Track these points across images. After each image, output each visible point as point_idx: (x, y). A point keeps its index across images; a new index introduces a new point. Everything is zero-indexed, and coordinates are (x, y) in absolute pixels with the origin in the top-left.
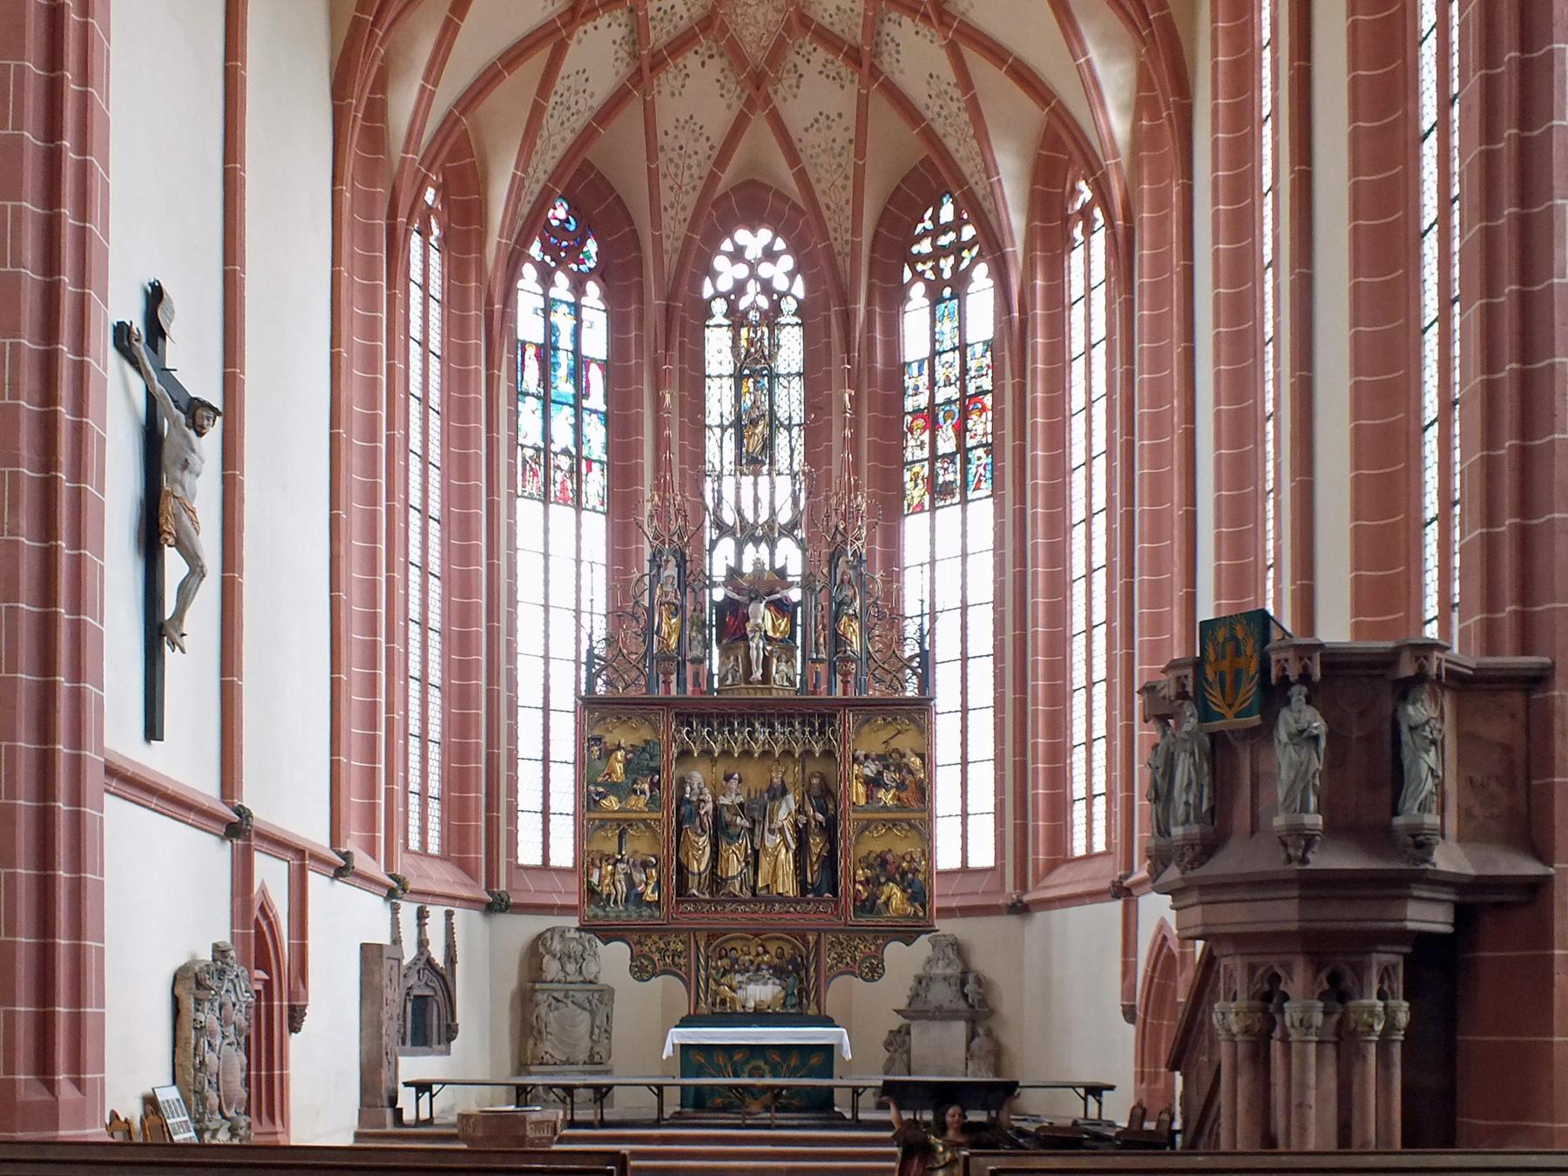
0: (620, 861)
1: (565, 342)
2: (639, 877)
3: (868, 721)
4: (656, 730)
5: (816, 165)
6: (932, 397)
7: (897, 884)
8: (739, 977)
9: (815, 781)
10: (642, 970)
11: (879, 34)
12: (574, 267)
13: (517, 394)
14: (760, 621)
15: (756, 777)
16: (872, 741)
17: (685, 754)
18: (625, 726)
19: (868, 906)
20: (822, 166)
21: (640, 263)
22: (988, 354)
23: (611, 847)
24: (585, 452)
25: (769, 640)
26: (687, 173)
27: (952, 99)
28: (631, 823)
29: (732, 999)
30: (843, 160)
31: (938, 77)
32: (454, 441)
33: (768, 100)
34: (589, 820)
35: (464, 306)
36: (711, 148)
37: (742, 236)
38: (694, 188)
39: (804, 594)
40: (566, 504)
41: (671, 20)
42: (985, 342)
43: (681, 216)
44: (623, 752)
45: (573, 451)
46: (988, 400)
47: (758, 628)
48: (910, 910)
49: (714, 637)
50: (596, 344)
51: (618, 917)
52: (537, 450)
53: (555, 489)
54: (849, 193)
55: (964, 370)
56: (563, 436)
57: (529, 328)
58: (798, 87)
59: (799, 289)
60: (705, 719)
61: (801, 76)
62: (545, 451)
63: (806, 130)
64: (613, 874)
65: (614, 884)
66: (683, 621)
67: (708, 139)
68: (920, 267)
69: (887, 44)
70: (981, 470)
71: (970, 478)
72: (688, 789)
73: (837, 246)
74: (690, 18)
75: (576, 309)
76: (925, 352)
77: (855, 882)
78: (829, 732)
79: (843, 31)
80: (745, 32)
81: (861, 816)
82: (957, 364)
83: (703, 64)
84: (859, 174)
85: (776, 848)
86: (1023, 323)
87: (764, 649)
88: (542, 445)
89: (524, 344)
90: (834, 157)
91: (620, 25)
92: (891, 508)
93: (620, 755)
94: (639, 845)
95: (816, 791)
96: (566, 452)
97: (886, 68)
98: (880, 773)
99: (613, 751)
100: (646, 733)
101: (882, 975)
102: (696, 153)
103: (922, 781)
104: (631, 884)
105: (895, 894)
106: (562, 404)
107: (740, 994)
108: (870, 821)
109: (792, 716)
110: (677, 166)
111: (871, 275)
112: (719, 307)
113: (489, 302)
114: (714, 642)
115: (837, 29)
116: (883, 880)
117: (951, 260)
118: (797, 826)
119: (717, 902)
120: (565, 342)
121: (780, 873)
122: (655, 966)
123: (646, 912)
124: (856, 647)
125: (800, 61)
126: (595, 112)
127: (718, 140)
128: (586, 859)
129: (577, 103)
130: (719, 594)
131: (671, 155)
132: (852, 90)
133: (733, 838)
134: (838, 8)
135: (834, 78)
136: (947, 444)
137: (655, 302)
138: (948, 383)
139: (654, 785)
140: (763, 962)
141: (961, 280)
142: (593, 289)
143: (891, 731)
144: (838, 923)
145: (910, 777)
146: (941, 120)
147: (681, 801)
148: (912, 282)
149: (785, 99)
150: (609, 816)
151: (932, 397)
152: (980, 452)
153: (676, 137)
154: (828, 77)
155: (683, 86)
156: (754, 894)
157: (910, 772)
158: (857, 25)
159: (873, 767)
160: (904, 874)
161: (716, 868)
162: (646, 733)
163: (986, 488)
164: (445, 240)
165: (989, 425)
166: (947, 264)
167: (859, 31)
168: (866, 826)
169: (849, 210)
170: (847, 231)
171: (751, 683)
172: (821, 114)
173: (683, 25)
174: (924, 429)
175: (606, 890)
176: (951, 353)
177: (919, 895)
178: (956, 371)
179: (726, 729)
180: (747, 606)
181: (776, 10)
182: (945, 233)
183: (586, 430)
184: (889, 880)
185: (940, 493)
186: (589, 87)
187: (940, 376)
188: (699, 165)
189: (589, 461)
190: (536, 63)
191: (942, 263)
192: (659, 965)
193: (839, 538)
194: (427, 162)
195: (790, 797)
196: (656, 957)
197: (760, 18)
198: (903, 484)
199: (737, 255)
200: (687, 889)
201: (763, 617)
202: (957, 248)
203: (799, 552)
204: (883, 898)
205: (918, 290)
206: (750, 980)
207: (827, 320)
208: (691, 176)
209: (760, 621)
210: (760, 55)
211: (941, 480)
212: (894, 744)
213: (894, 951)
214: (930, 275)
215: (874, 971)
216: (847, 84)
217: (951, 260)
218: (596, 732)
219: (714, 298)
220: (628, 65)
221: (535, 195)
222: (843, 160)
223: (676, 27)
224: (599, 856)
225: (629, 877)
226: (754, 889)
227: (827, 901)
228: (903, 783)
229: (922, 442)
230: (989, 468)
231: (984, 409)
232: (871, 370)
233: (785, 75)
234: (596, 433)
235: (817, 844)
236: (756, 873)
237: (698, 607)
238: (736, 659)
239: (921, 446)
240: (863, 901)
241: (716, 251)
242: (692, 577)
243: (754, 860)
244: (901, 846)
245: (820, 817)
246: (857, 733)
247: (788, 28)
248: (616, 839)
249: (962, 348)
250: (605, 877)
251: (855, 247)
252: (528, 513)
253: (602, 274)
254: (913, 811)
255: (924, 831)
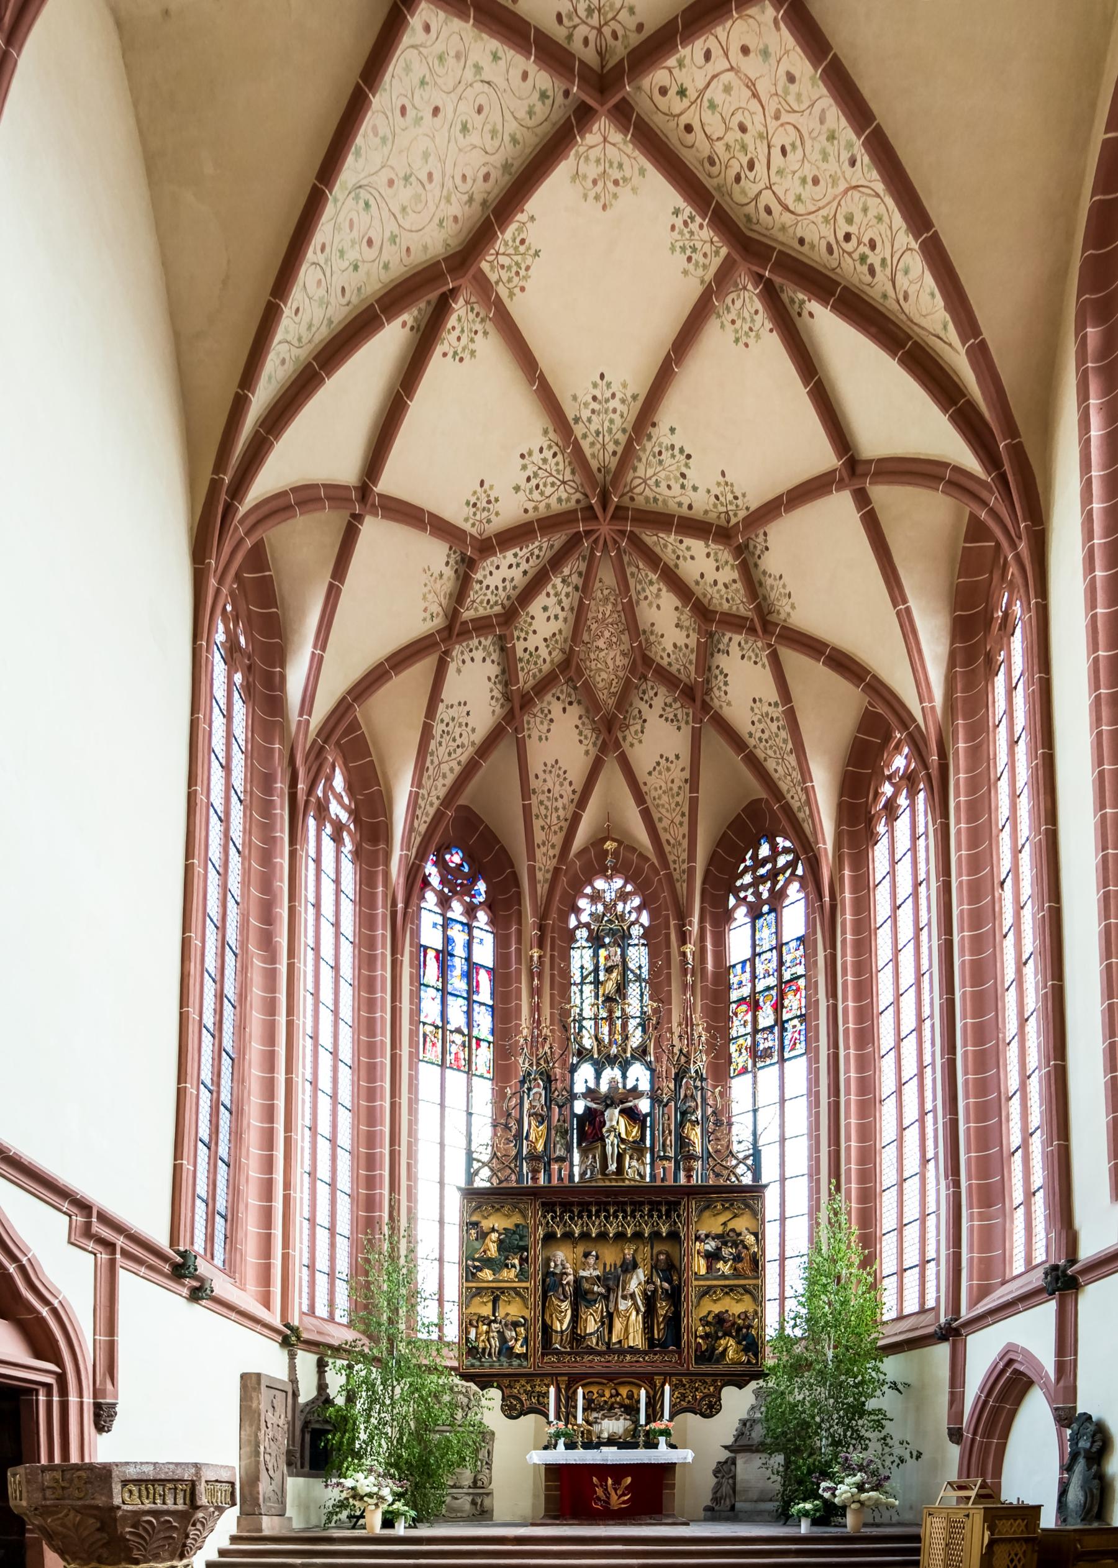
0: (495, 1321)
1: (459, 950)
2: (510, 1334)
3: (707, 1207)
4: (525, 1217)
5: (658, 806)
6: (754, 986)
7: (733, 1337)
8: (595, 1415)
9: (662, 1257)
10: (512, 1410)
11: (709, 669)
12: (467, 899)
13: (418, 983)
14: (614, 1123)
15: (611, 1256)
16: (713, 1224)
17: (549, 1238)
18: (499, 1214)
19: (708, 1356)
20: (663, 806)
21: (519, 896)
22: (801, 947)
23: (486, 1311)
24: (475, 1033)
25: (623, 1141)
26: (554, 815)
27: (772, 720)
28: (503, 1290)
29: (589, 1432)
30: (679, 799)
31: (760, 700)
32: (363, 1007)
33: (618, 745)
34: (467, 1288)
35: (372, 905)
36: (574, 792)
37: (600, 884)
38: (561, 828)
39: (652, 1107)
40: (459, 1070)
41: (536, 663)
42: (797, 939)
43: (551, 853)
44: (497, 1235)
45: (466, 1031)
46: (802, 982)
47: (613, 1129)
48: (744, 1358)
49: (575, 1141)
50: (484, 954)
51: (491, 1367)
52: (437, 1027)
53: (449, 1058)
54: (685, 829)
55: (781, 963)
56: (457, 1018)
57: (431, 937)
58: (642, 732)
59: (645, 918)
60: (567, 1207)
61: (645, 721)
62: (443, 1026)
63: (650, 773)
64: (487, 1333)
65: (488, 1340)
66: (549, 1129)
67: (571, 783)
68: (742, 895)
69: (716, 677)
70: (796, 1035)
71: (786, 1042)
72: (552, 1264)
73: (676, 876)
74: (552, 661)
75: (469, 927)
76: (748, 954)
77: (696, 1337)
78: (674, 1215)
79: (679, 670)
80: (598, 679)
81: (702, 1283)
82: (775, 959)
83: (564, 710)
84: (694, 803)
85: (627, 1310)
86: (833, 908)
87: (618, 1146)
88: (440, 1024)
89: (426, 948)
90: (673, 796)
91: (493, 662)
92: (721, 1070)
93: (494, 1236)
94: (512, 1310)
95: (662, 1265)
96: (458, 1031)
97: (716, 703)
98: (719, 1249)
99: (488, 1234)
100: (517, 1219)
101: (720, 1410)
102: (562, 797)
103: (755, 1254)
104: (503, 1339)
105: (730, 1347)
106: (457, 996)
107: (596, 1428)
108: (710, 1287)
109: (642, 1204)
110: (547, 808)
111: (702, 901)
112: (582, 934)
113: (394, 904)
114: (575, 1145)
115: (673, 669)
116: (720, 1334)
117: (769, 884)
118: (646, 1294)
119: (577, 1354)
120: (459, 950)
121: (631, 1330)
122: (522, 1405)
123: (516, 1362)
124: (698, 1149)
125: (644, 707)
126: (476, 747)
127: (578, 786)
128: (467, 1323)
129: (461, 735)
130: (579, 1107)
131: (542, 797)
132: (687, 730)
133: (591, 1303)
134: (675, 646)
135: (672, 721)
136: (766, 1018)
137: (530, 919)
138: (767, 974)
139: (523, 1261)
140: (616, 1402)
141: (777, 899)
142: (482, 917)
143: (728, 1215)
144: (683, 1369)
145: (745, 1251)
146: (762, 745)
147: (547, 1274)
148: (736, 907)
149: (632, 745)
150: (485, 1285)
151: (754, 986)
152: (796, 1022)
153: (545, 781)
154: (667, 719)
155: (549, 731)
156: (608, 1348)
157: (746, 1247)
158: (691, 662)
159: (713, 1244)
160: (739, 1329)
161: (576, 1328)
162: (517, 1219)
163: (801, 1048)
164: (357, 854)
165: (803, 1001)
166: (764, 890)
167: (692, 668)
168: (706, 1292)
169: (685, 843)
170: (683, 861)
171: (607, 1175)
172: (662, 756)
173: (546, 668)
174: (747, 1012)
175: (481, 1345)
176: (769, 953)
177: (752, 1345)
178: (774, 965)
179: (585, 1215)
180: (603, 1114)
181: (623, 654)
182: (763, 866)
183: (476, 1016)
184: (726, 1334)
185: (761, 1057)
186: (469, 720)
187: (760, 970)
188: (564, 808)
189: (478, 1040)
190: (422, 670)
191: (761, 888)
192: (527, 1404)
193: (683, 1059)
194: (323, 735)
195: (640, 1271)
196: (524, 1397)
197: (610, 663)
198: (730, 1055)
199: (596, 897)
200: (551, 1344)
201: (614, 1118)
202: (774, 875)
203: (648, 1073)
204: (721, 1349)
205: (741, 914)
206: (604, 1417)
207: (668, 936)
208: (558, 818)
209: (614, 1123)
210: (610, 701)
211: (761, 1047)
212: (730, 1226)
213: (729, 1394)
214: (751, 899)
215: (711, 1408)
216: (683, 725)
217: (769, 884)
218: (474, 1219)
219: (577, 927)
220: (502, 706)
221: (430, 817)
222: (679, 799)
223: (540, 671)
224: (476, 1318)
225: (501, 1334)
226: (608, 1344)
227: (672, 1352)
228: (740, 1253)
229: (745, 1022)
230: (803, 1033)
231: (798, 989)
232: (703, 970)
233: (632, 722)
234: (484, 1022)
235: (663, 1308)
236: (610, 1332)
237: (562, 1118)
238: (594, 1157)
239: (745, 1025)
240: (702, 1352)
241: (579, 893)
242: (556, 1093)
243: (608, 1320)
244: (735, 1307)
245: (666, 1285)
246: (699, 1216)
247: (633, 669)
248: (490, 1305)
249: (779, 947)
250: (481, 1334)
251: (691, 871)
252: (428, 1075)
253: (490, 905)
254: (746, 1278)
255: (756, 1294)
